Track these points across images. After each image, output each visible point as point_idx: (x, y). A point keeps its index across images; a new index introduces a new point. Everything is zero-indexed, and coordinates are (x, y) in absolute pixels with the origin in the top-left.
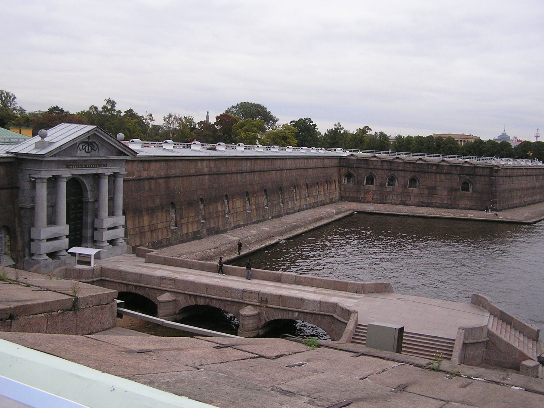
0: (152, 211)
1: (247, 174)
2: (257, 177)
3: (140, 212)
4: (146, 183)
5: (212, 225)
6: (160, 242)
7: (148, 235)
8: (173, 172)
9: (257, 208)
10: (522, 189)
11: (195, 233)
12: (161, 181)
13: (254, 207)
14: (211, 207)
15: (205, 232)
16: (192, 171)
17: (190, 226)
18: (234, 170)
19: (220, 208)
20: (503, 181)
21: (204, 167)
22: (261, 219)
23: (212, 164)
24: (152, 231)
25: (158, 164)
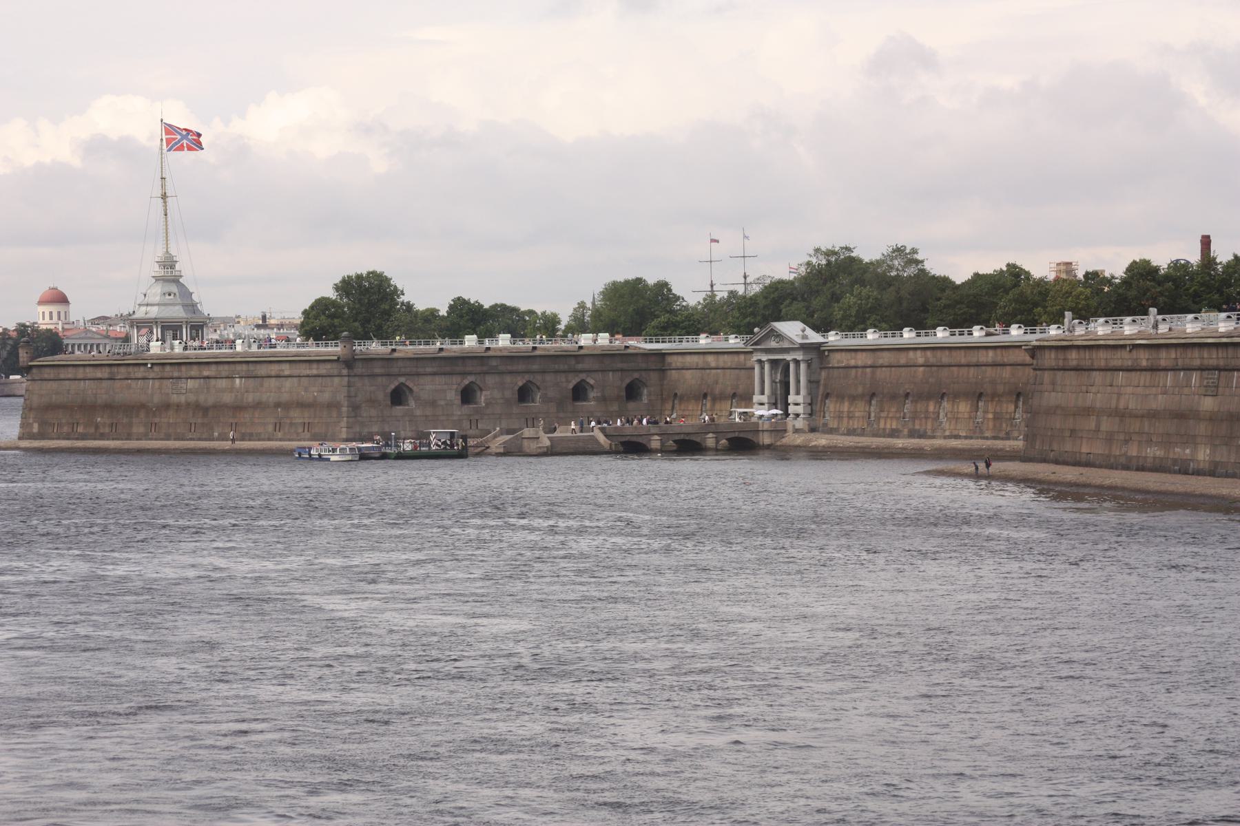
0: (853, 398)
1: (989, 369)
2: (1006, 373)
3: (843, 398)
4: (854, 371)
5: (917, 427)
6: (855, 430)
7: (845, 420)
8: (881, 362)
9: (994, 418)
10: (1122, 415)
11: (893, 430)
12: (868, 370)
13: (990, 416)
14: (919, 406)
15: (906, 432)
16: (903, 361)
17: (889, 421)
18: (963, 361)
19: (931, 408)
20: (1053, 383)
21: (919, 358)
22: (1002, 435)
23: (929, 353)
24: (849, 418)
25: (864, 354)
